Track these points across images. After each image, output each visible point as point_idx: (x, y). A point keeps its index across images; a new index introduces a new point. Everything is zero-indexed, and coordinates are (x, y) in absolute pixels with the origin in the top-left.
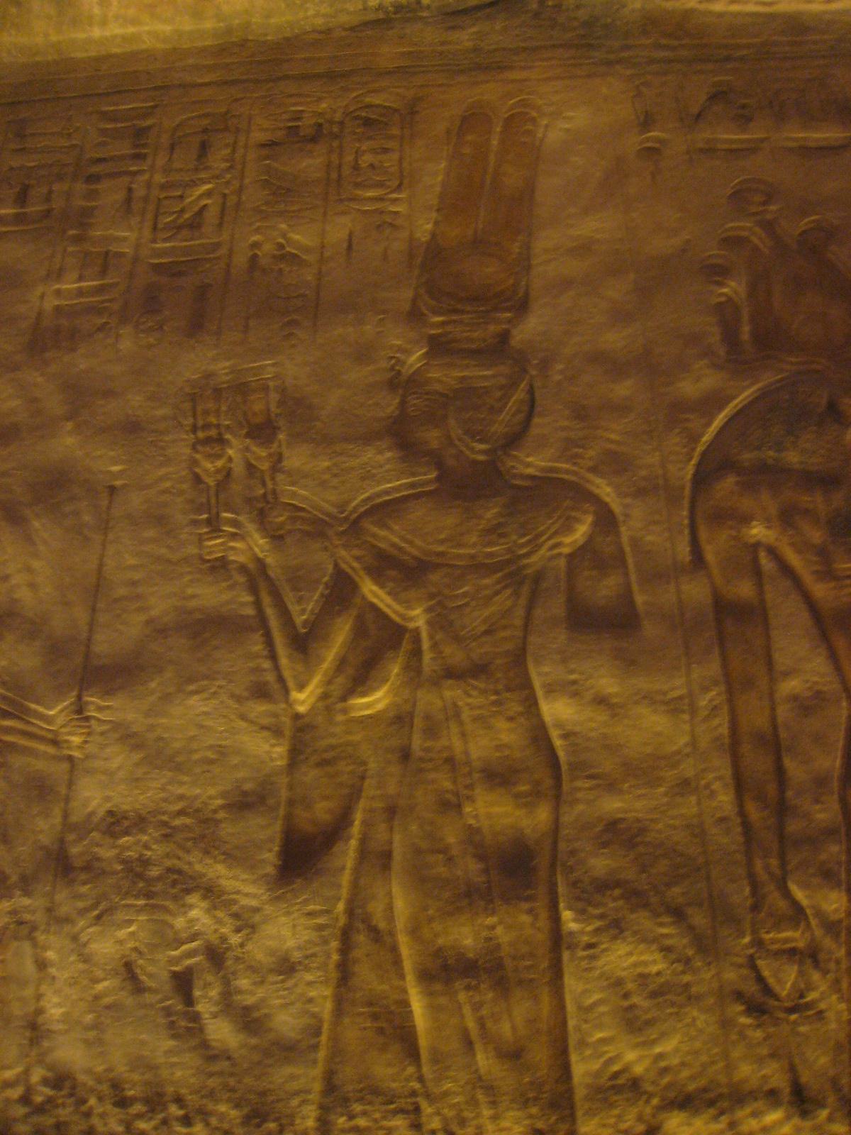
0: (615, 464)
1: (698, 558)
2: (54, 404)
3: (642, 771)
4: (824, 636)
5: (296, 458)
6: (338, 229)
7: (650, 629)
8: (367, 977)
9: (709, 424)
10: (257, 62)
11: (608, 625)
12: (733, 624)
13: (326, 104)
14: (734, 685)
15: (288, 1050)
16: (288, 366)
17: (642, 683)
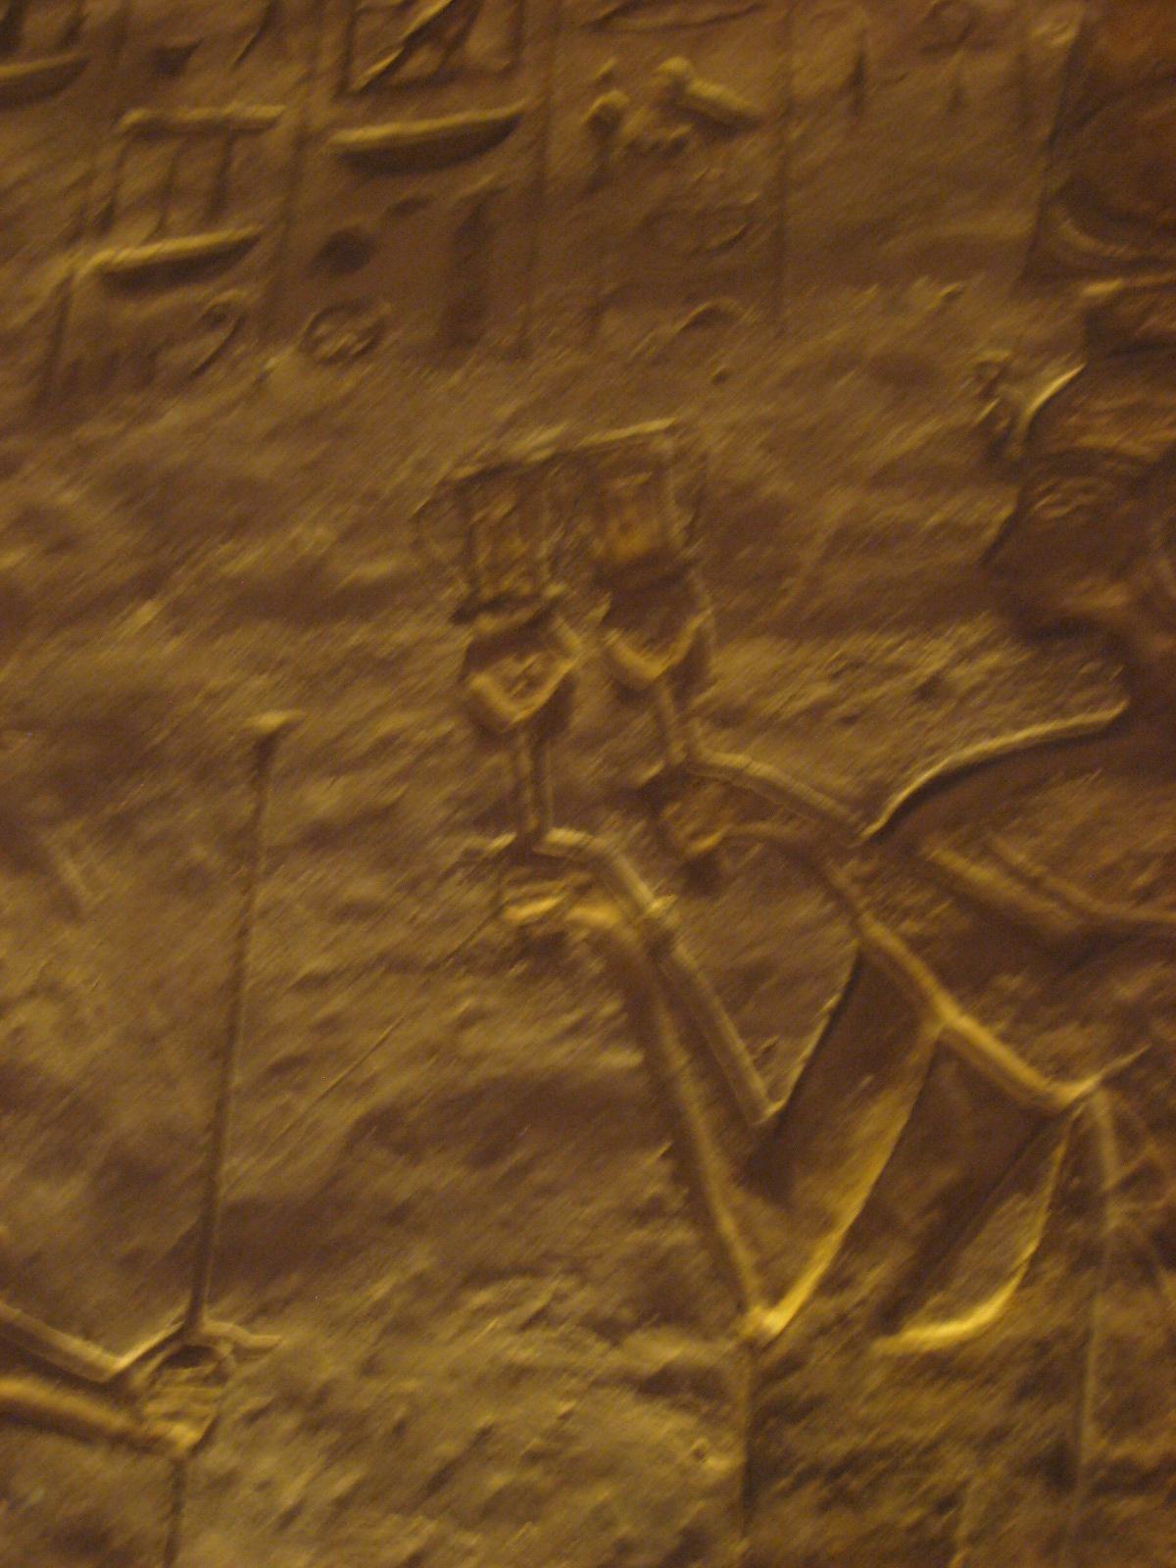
2: (111, 541)
5: (738, 667)
16: (712, 423)
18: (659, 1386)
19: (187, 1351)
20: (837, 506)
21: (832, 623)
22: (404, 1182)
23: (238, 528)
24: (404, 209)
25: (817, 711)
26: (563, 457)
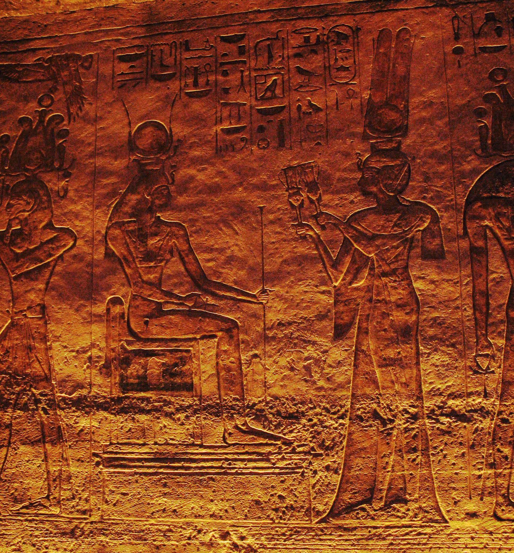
0: (438, 198)
1: (466, 234)
2: (233, 178)
3: (445, 303)
4: (507, 260)
5: (326, 198)
7: (449, 258)
8: (363, 367)
11: (434, 256)
12: (477, 256)
13: (319, 27)
14: (475, 276)
15: (341, 386)
16: (320, 161)
17: (446, 277)
18: (323, 293)
19: (264, 291)
20: (338, 174)
21: (337, 192)
22: (290, 269)
23: (253, 176)
24: (269, 122)
25: (337, 204)
26: (299, 166)
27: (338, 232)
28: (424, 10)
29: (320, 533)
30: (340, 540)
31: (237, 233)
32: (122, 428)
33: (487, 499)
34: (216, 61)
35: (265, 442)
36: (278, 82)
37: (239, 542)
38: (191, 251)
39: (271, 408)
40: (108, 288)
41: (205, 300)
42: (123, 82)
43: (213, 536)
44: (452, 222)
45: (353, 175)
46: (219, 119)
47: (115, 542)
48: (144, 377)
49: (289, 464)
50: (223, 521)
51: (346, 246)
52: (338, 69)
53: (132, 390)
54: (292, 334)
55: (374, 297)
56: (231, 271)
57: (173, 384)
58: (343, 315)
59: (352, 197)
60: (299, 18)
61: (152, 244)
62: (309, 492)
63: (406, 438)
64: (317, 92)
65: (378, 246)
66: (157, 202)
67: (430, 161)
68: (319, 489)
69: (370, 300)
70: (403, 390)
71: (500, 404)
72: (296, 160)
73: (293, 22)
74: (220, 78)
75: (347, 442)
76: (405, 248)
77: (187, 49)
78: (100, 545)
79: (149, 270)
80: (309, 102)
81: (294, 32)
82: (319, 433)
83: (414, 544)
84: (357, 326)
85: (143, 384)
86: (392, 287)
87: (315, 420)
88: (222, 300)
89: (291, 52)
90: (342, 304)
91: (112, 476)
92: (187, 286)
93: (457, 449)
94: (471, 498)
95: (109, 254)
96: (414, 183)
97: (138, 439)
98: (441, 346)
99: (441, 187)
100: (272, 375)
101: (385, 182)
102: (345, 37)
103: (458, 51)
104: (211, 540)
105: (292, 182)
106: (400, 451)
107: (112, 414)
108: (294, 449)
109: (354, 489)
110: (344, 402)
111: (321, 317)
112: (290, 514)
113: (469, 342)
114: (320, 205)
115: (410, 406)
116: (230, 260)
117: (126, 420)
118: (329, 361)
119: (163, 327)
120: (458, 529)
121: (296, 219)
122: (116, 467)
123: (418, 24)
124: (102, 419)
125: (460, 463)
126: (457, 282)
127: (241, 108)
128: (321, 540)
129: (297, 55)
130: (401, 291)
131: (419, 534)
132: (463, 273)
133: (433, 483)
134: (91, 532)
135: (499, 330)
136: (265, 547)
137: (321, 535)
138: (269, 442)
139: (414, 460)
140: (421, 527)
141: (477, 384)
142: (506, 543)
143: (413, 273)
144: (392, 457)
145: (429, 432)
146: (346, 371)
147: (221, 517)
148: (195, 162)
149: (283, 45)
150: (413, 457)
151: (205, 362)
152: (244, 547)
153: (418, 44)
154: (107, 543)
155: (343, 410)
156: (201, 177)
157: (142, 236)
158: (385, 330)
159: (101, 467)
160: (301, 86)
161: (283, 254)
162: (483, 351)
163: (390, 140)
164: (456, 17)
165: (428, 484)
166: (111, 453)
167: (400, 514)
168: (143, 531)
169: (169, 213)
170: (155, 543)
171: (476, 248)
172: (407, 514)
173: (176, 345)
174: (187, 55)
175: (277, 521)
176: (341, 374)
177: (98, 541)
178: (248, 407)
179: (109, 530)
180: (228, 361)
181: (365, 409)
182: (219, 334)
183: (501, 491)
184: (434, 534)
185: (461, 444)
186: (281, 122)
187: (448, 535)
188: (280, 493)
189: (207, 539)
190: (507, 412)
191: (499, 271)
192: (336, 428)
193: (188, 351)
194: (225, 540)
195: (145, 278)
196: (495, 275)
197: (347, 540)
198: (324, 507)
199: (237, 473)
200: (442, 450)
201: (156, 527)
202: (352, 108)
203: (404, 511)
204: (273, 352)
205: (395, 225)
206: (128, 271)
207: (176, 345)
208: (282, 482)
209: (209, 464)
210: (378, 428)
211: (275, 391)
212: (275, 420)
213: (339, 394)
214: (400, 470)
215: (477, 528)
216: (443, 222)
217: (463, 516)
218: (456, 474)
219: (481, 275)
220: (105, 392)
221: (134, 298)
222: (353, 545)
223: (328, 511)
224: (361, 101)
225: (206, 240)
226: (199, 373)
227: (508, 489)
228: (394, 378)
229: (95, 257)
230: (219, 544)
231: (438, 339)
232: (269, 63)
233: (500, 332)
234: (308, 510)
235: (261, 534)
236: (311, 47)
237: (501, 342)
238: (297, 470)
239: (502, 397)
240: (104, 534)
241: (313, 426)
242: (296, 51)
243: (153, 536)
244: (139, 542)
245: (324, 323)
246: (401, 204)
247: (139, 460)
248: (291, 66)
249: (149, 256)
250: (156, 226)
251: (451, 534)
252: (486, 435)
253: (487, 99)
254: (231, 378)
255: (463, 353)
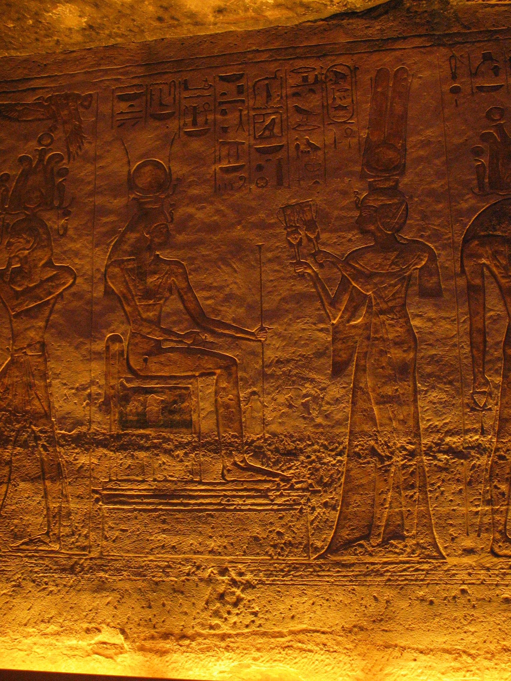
0: (436, 236)
1: (463, 272)
3: (442, 341)
4: (503, 298)
5: (324, 236)
6: (331, 134)
7: (446, 296)
8: (361, 404)
9: (470, 220)
10: (284, 44)
11: (432, 294)
12: (474, 293)
13: (317, 67)
14: (472, 314)
15: (339, 423)
16: (317, 199)
17: (444, 314)
18: (321, 330)
19: (262, 329)
20: (336, 213)
24: (267, 161)
25: (335, 243)
27: (336, 270)
28: (421, 50)
29: (318, 569)
30: (338, 576)
31: (235, 271)
32: (121, 465)
33: (484, 535)
34: (215, 99)
35: (263, 479)
36: (277, 121)
37: (238, 578)
38: (189, 288)
39: (270, 445)
40: (108, 325)
41: (204, 337)
42: (122, 122)
43: (212, 572)
44: (450, 260)
45: (351, 214)
46: (218, 157)
47: (114, 578)
48: (144, 414)
49: (288, 501)
50: (222, 557)
51: (344, 284)
52: (336, 109)
53: (131, 427)
54: (290, 371)
55: (372, 335)
56: (230, 308)
57: (172, 421)
58: (341, 353)
59: (350, 236)
60: (297, 58)
61: (151, 282)
62: (307, 528)
63: (403, 474)
64: (315, 131)
65: (376, 284)
66: (156, 240)
67: (428, 199)
68: (317, 526)
69: (368, 338)
70: (401, 427)
71: (497, 441)
72: (294, 199)
73: (291, 62)
74: (219, 117)
75: (345, 479)
76: (402, 286)
77: (186, 89)
78: (99, 581)
79: (148, 308)
80: (308, 140)
81: (292, 71)
82: (317, 470)
83: (412, 580)
84: (354, 363)
85: (143, 421)
86: (389, 324)
87: (313, 457)
88: (220, 338)
89: (290, 91)
90: (340, 342)
91: (111, 512)
92: (186, 324)
93: (454, 486)
94: (468, 535)
95: (108, 292)
96: (412, 222)
97: (137, 476)
98: (439, 383)
99: (439, 225)
100: (270, 412)
101: (383, 220)
102: (343, 77)
103: (455, 91)
104: (210, 576)
105: (290, 220)
106: (398, 487)
107: (111, 451)
108: (292, 486)
109: (352, 526)
110: (342, 439)
111: (319, 355)
112: (288, 550)
113: (466, 379)
114: (318, 243)
115: (408, 443)
116: (229, 298)
117: (125, 457)
118: (327, 398)
119: (162, 364)
120: (455, 565)
121: (294, 258)
122: (115, 503)
123: (415, 63)
124: (101, 456)
125: (458, 500)
126: (455, 320)
127: (239, 147)
128: (319, 576)
129: (295, 95)
130: (399, 329)
131: (417, 570)
132: (460, 310)
133: (431, 519)
134: (91, 568)
135: (496, 367)
136: (262, 583)
137: (319, 571)
138: (268, 479)
139: (412, 496)
140: (419, 563)
141: (475, 421)
142: (503, 579)
143: (411, 311)
144: (390, 494)
145: (427, 469)
146: (344, 408)
147: (220, 553)
148: (193, 200)
149: (281, 84)
150: (411, 494)
151: (204, 400)
152: (242, 583)
153: (415, 83)
154: (107, 579)
155: (341, 447)
156: (200, 215)
157: (141, 274)
158: (383, 368)
159: (100, 503)
160: (299, 125)
161: (281, 292)
162: (480, 388)
163: (387, 179)
164: (453, 56)
165: (425, 521)
166: (110, 489)
167: (397, 550)
168: (143, 567)
169: (168, 251)
170: (154, 579)
171: (474, 286)
172: (405, 551)
173: (175, 382)
174: (185, 95)
175: (275, 557)
176: (339, 411)
177: (97, 577)
178: (246, 443)
179: (108, 566)
180: (228, 398)
181: (363, 446)
182: (218, 371)
183: (498, 527)
184: (431, 570)
185: (458, 480)
186: (279, 160)
187: (446, 571)
188: (278, 529)
189: (206, 574)
190: (504, 449)
191: (496, 309)
192: (334, 465)
193: (187, 389)
194: (224, 576)
195: (144, 316)
196: (492, 313)
197: (344, 576)
198: (322, 543)
199: (235, 510)
200: (439, 487)
201: (155, 563)
202: (350, 147)
203: (402, 547)
204: (272, 389)
205: (393, 263)
206: (128, 309)
207: (175, 382)
208: (281, 518)
209: (207, 501)
210: (375, 464)
211: (273, 428)
212: (274, 457)
213: (337, 431)
214: (397, 507)
215: (474, 564)
216: (441, 260)
217: (460, 552)
218: (454, 510)
219: (478, 313)
220: (104, 429)
221: (133, 335)
222: (351, 581)
223: (326, 547)
224: (359, 140)
225: (205, 278)
226: (199, 410)
227: (505, 525)
228: (391, 415)
229: (95, 295)
230: (217, 580)
231: (435, 376)
232: (267, 102)
233: (497, 370)
234: (307, 546)
235: (259, 570)
236: (310, 86)
237: (498, 380)
238: (295, 507)
239: (499, 434)
240: (103, 570)
241: (311, 463)
242: (294, 90)
243: (152, 572)
244: (138, 578)
245: (322, 360)
246: (398, 242)
247: (138, 496)
248: (289, 106)
249: (148, 294)
250: (155, 265)
251: (448, 570)
252: (483, 471)
253: (484, 138)
254: (230, 415)
255: (460, 391)
